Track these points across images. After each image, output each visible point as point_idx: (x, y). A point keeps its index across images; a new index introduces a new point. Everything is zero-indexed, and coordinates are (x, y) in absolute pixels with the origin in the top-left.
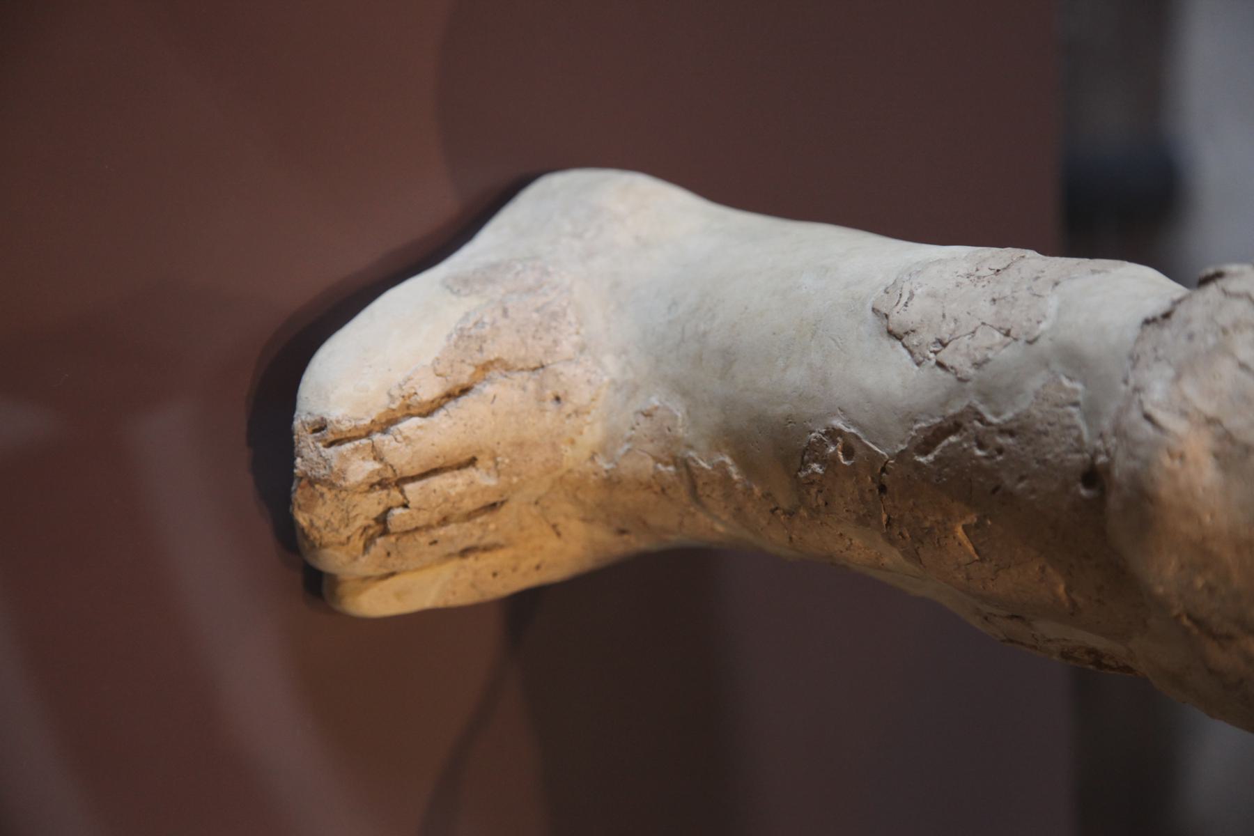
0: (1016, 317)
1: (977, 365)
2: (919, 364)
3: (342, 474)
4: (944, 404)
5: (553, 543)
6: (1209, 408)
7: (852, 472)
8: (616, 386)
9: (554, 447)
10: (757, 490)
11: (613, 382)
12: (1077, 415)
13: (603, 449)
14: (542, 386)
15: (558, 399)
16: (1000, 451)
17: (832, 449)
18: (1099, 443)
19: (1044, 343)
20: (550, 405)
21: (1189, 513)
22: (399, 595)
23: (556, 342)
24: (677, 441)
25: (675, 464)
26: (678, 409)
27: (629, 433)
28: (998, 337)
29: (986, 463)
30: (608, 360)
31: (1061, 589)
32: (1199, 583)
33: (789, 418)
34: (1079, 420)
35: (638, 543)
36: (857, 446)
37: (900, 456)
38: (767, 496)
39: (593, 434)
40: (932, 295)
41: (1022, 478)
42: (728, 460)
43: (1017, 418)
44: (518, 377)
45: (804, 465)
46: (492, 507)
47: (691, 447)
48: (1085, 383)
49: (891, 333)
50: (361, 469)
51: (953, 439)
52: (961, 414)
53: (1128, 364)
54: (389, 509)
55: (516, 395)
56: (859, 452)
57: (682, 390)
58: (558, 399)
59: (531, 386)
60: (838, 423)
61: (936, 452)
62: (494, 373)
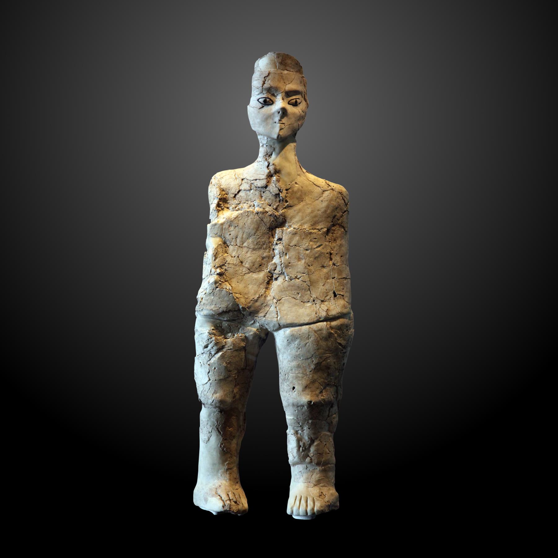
0: (206, 423)
1: (211, 427)
2: (212, 435)
3: (229, 504)
4: (215, 431)
5: (239, 490)
6: (212, 395)
7: (225, 444)
8: (218, 480)
9: (226, 486)
10: (229, 459)
11: (218, 480)
12: (215, 414)
13: (226, 481)
14: (219, 488)
15: (220, 486)
16: (220, 423)
17: (222, 447)
18: (217, 411)
19: (208, 419)
20: (221, 487)
21: (222, 396)
22: (245, 503)
23: (213, 488)
24: (224, 471)
25: (227, 471)
26: (220, 471)
27: (224, 478)
28: (208, 425)
29: (221, 425)
30: (215, 482)
31: (235, 417)
32: (229, 396)
33: (220, 454)
34: (215, 414)
35: (238, 480)
36: (221, 443)
37: (222, 436)
38: (229, 458)
39: (224, 482)
40: (204, 436)
41: (222, 420)
42: (226, 463)
43: (216, 421)
44: (217, 490)
45: (225, 451)
46: (234, 493)
47: (225, 469)
48: (211, 414)
49: (209, 440)
50: (228, 502)
51: (219, 429)
52: (216, 428)
53: (209, 408)
54: (234, 501)
55: (219, 490)
56: (222, 442)
57: (218, 471)
58: (220, 486)
59: (218, 489)
60: (219, 445)
61: (220, 431)
62: (217, 493)
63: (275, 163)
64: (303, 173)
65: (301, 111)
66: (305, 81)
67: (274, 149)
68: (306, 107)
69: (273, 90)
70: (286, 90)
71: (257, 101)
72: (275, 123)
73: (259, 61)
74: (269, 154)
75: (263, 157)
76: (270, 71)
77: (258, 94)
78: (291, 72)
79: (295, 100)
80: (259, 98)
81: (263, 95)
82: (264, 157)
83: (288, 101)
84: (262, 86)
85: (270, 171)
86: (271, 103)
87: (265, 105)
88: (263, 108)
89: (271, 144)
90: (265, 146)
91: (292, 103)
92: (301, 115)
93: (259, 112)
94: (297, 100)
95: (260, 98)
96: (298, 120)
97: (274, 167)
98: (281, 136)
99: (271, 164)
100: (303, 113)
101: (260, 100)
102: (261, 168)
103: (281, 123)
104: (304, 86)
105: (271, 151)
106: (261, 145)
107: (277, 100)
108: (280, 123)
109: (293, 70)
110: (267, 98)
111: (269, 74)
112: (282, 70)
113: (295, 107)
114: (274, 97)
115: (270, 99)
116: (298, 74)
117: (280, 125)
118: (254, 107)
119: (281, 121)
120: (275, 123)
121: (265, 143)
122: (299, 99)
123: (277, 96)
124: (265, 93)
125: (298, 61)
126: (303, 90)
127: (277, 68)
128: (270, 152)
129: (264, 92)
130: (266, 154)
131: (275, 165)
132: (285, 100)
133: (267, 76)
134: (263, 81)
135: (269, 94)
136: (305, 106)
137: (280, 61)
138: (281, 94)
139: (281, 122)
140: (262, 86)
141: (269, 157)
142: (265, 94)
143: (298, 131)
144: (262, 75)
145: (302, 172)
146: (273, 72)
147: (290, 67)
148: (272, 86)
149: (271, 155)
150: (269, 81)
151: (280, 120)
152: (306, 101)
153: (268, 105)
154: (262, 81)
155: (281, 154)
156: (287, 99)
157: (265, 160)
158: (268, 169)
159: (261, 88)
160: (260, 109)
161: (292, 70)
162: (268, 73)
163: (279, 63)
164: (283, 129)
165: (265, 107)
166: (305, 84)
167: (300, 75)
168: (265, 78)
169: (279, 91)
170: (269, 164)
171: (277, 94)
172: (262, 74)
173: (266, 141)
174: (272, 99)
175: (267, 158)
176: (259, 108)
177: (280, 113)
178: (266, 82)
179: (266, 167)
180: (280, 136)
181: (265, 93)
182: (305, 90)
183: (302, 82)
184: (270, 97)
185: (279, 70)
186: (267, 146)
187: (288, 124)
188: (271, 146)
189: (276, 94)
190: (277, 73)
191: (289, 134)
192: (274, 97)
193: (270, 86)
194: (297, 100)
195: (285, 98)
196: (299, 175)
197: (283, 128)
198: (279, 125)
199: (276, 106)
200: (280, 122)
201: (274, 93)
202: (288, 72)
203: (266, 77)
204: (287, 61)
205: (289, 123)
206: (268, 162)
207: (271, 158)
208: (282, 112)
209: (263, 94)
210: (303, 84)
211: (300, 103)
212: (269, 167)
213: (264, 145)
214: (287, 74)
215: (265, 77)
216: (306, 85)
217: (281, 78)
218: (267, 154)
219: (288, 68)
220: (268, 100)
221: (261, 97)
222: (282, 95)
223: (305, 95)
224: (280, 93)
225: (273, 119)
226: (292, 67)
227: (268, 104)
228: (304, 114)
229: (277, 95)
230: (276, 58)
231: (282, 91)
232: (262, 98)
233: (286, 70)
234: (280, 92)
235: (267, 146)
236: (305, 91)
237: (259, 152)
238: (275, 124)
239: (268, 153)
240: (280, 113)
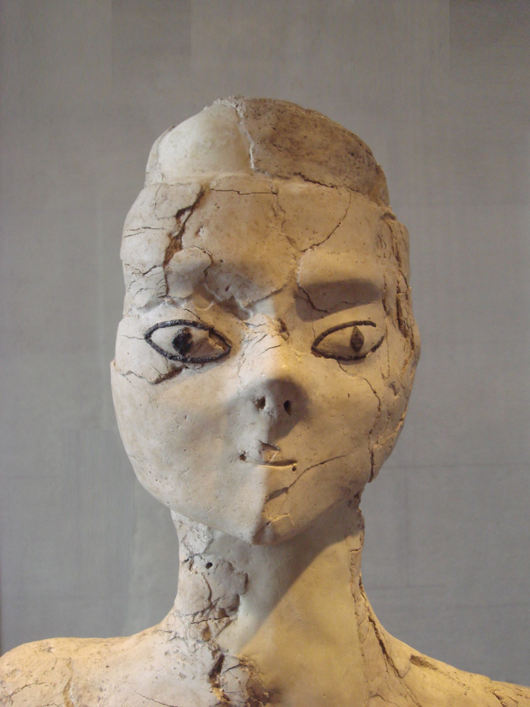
63: (253, 657)
64: (397, 680)
65: (380, 385)
66: (399, 236)
67: (247, 581)
68: (406, 363)
69: (223, 279)
70: (299, 280)
71: (144, 341)
72: (243, 457)
73: (159, 142)
74: (220, 605)
75: (190, 618)
76: (212, 179)
77: (148, 306)
78: (323, 188)
79: (349, 331)
80: (152, 324)
81: (173, 309)
82: (198, 618)
83: (311, 339)
84: (166, 262)
85: (224, 696)
86: (219, 348)
87: (184, 360)
88: (174, 379)
89: (228, 557)
90: (199, 564)
91: (339, 346)
92: (383, 408)
93: (153, 400)
94: (362, 329)
95: (156, 328)
96: (371, 432)
97: (247, 677)
98: (274, 527)
99: (229, 663)
100: (395, 394)
101: (156, 337)
102: (183, 676)
103: (272, 460)
104: (393, 258)
105: (232, 592)
106: (183, 555)
107: (248, 333)
108: (267, 463)
109: (338, 181)
110: (194, 324)
111: (201, 196)
112: (274, 176)
113: (351, 368)
114: (236, 315)
115: (212, 332)
116: (362, 201)
117: (270, 474)
118: (130, 373)
119: (275, 448)
120: (243, 457)
121: (199, 546)
122: (374, 325)
123: (252, 314)
124: (182, 299)
125: (361, 144)
126: (390, 281)
127: (248, 165)
128: (224, 597)
129: (177, 293)
130: (206, 604)
131: (251, 667)
132: (296, 334)
133: (192, 208)
134: (170, 235)
135: (203, 301)
136: (404, 356)
137: (267, 130)
138: (269, 304)
139: (275, 456)
140: (162, 259)
141: (220, 619)
142: (183, 305)
143: (368, 486)
144: (165, 205)
145: (392, 672)
146: (222, 187)
147: (320, 163)
148: (217, 258)
149: (234, 608)
150: (204, 234)
151: (266, 446)
152: (405, 335)
153: (203, 362)
154: (165, 232)
155: (283, 604)
156: (308, 324)
157: (200, 638)
158: (217, 686)
159: (160, 269)
160: (158, 382)
161: (329, 179)
162: (197, 189)
163: (262, 141)
164: (286, 490)
165: (184, 371)
166: (401, 249)
167: (374, 205)
168: (183, 218)
169: (262, 287)
170: (222, 658)
171: (249, 300)
172: (165, 197)
173: (206, 540)
174: (221, 327)
175: (211, 624)
176: (155, 377)
177: (269, 404)
178: (185, 240)
179: (206, 677)
180: (268, 531)
181: (182, 299)
182: (401, 278)
183: (386, 239)
184: (209, 319)
185: (260, 174)
186: (209, 565)
187: (317, 459)
188: (231, 568)
189: (241, 304)
190: (247, 191)
191: (323, 506)
192: (235, 320)
193: (206, 257)
194: (362, 328)
195: (298, 320)
196: (377, 695)
197: (287, 485)
198: (261, 470)
199: (244, 367)
200: (265, 455)
201: (232, 298)
202: (312, 185)
203: (187, 213)
204: (303, 133)
205: (322, 454)
206: (214, 653)
207: (231, 628)
208: (276, 399)
209: (173, 303)
210: (389, 248)
211: (374, 349)
212: (221, 677)
213: (196, 558)
214: (303, 196)
215: (180, 213)
216: (402, 254)
217: (271, 214)
218: (211, 607)
219: (307, 167)
220: (197, 334)
221: (159, 321)
222: (276, 310)
223: (402, 305)
224: (267, 297)
225: (229, 440)
226: (332, 164)
227: (199, 355)
228: (397, 396)
229: (250, 306)
230: (246, 117)
231: (279, 285)
232: (164, 325)
233: (297, 178)
234: (267, 293)
235: (209, 565)
236: (402, 284)
237: (179, 591)
238: (241, 464)
239: (212, 600)
240: (269, 404)
